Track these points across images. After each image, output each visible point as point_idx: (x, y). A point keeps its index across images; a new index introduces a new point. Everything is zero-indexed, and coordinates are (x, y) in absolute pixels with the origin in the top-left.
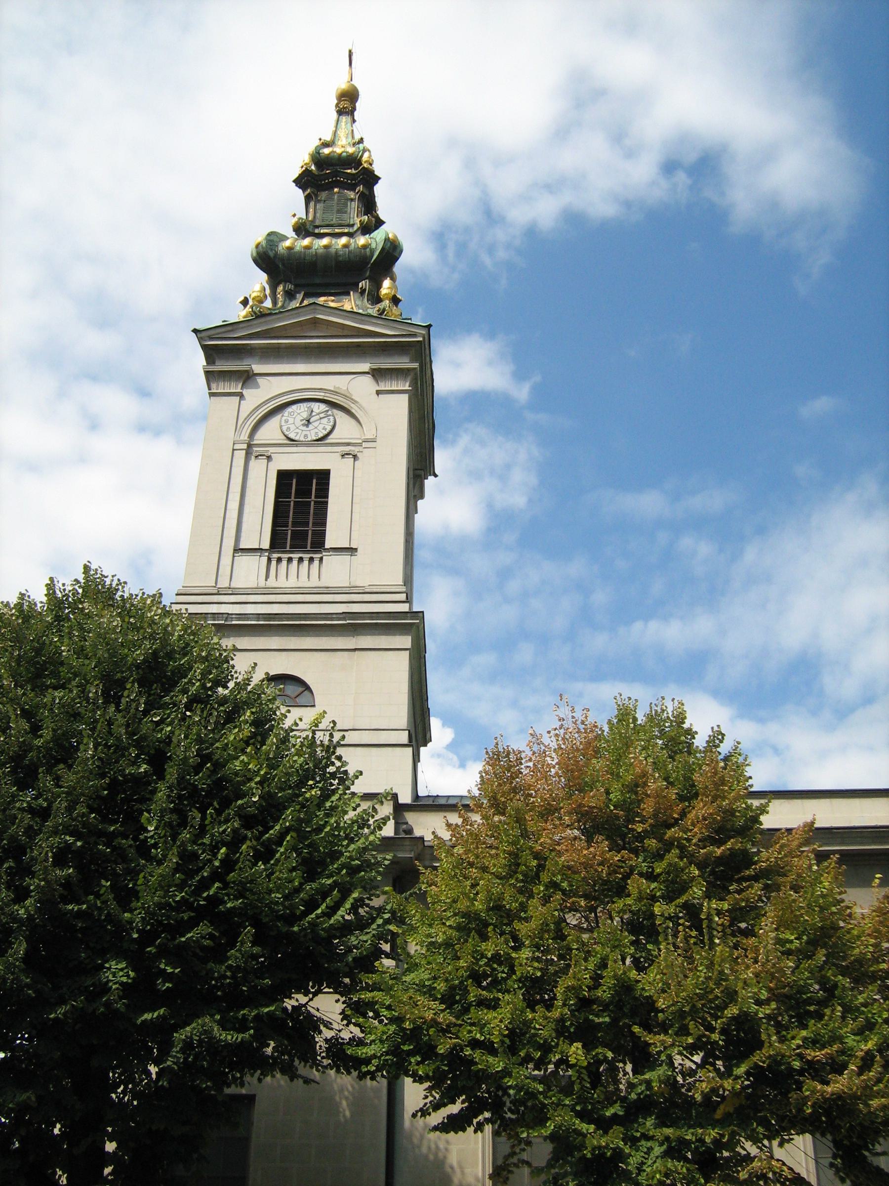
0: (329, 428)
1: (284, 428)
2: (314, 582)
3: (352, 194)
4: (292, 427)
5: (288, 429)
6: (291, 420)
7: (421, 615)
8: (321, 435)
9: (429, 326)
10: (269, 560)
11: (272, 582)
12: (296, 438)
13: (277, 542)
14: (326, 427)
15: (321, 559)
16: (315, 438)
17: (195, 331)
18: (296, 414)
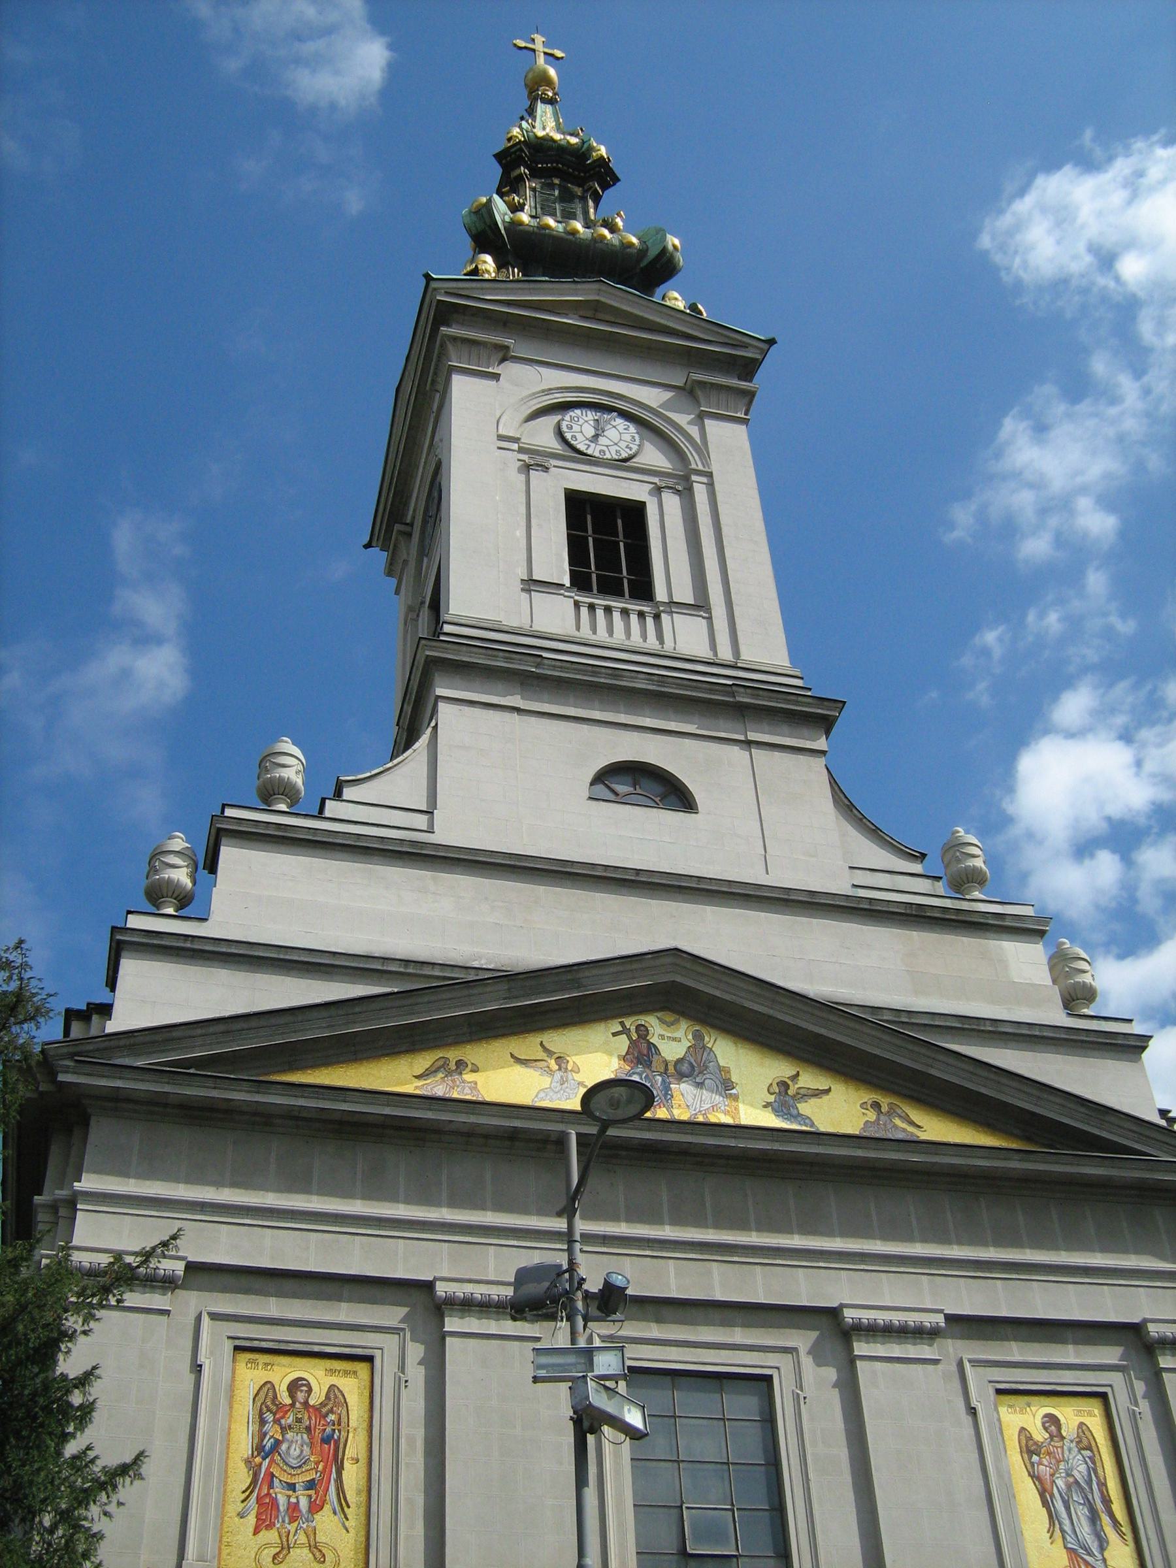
0: (635, 448)
1: (568, 436)
2: (652, 643)
3: (578, 191)
4: (579, 436)
5: (574, 437)
6: (576, 428)
7: (841, 705)
8: (624, 455)
9: (771, 342)
10: (577, 605)
11: (585, 633)
12: (589, 452)
13: (580, 582)
14: (631, 445)
15: (657, 617)
16: (617, 457)
17: (428, 277)
18: (581, 421)
